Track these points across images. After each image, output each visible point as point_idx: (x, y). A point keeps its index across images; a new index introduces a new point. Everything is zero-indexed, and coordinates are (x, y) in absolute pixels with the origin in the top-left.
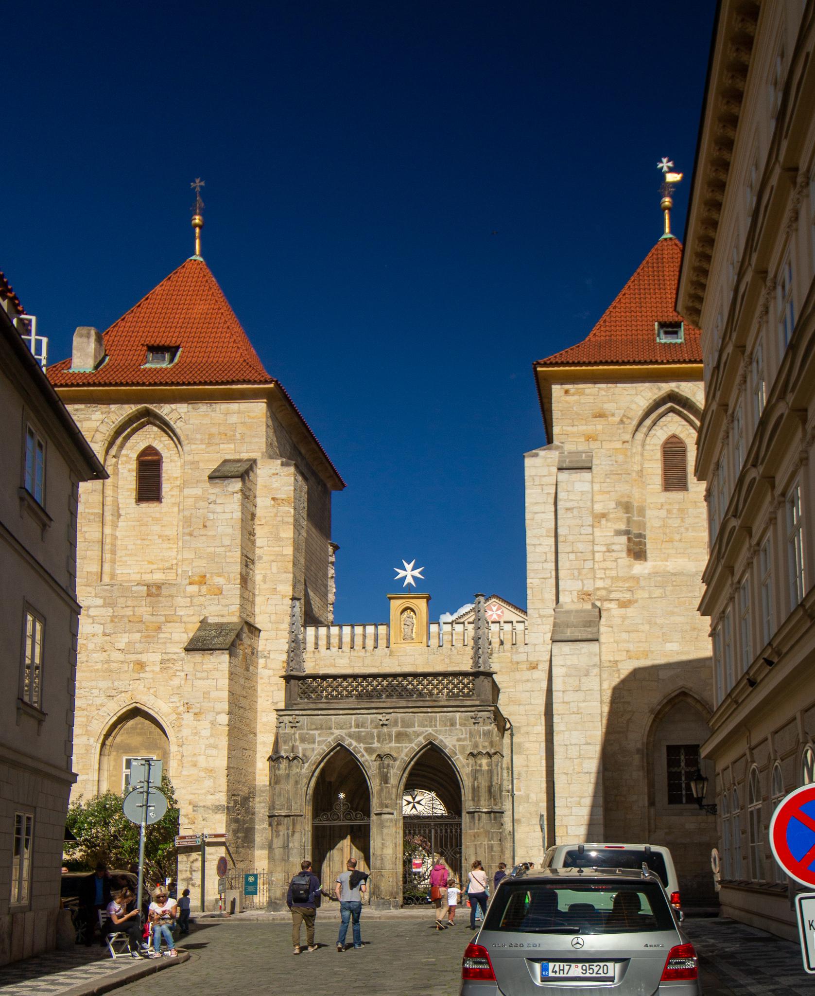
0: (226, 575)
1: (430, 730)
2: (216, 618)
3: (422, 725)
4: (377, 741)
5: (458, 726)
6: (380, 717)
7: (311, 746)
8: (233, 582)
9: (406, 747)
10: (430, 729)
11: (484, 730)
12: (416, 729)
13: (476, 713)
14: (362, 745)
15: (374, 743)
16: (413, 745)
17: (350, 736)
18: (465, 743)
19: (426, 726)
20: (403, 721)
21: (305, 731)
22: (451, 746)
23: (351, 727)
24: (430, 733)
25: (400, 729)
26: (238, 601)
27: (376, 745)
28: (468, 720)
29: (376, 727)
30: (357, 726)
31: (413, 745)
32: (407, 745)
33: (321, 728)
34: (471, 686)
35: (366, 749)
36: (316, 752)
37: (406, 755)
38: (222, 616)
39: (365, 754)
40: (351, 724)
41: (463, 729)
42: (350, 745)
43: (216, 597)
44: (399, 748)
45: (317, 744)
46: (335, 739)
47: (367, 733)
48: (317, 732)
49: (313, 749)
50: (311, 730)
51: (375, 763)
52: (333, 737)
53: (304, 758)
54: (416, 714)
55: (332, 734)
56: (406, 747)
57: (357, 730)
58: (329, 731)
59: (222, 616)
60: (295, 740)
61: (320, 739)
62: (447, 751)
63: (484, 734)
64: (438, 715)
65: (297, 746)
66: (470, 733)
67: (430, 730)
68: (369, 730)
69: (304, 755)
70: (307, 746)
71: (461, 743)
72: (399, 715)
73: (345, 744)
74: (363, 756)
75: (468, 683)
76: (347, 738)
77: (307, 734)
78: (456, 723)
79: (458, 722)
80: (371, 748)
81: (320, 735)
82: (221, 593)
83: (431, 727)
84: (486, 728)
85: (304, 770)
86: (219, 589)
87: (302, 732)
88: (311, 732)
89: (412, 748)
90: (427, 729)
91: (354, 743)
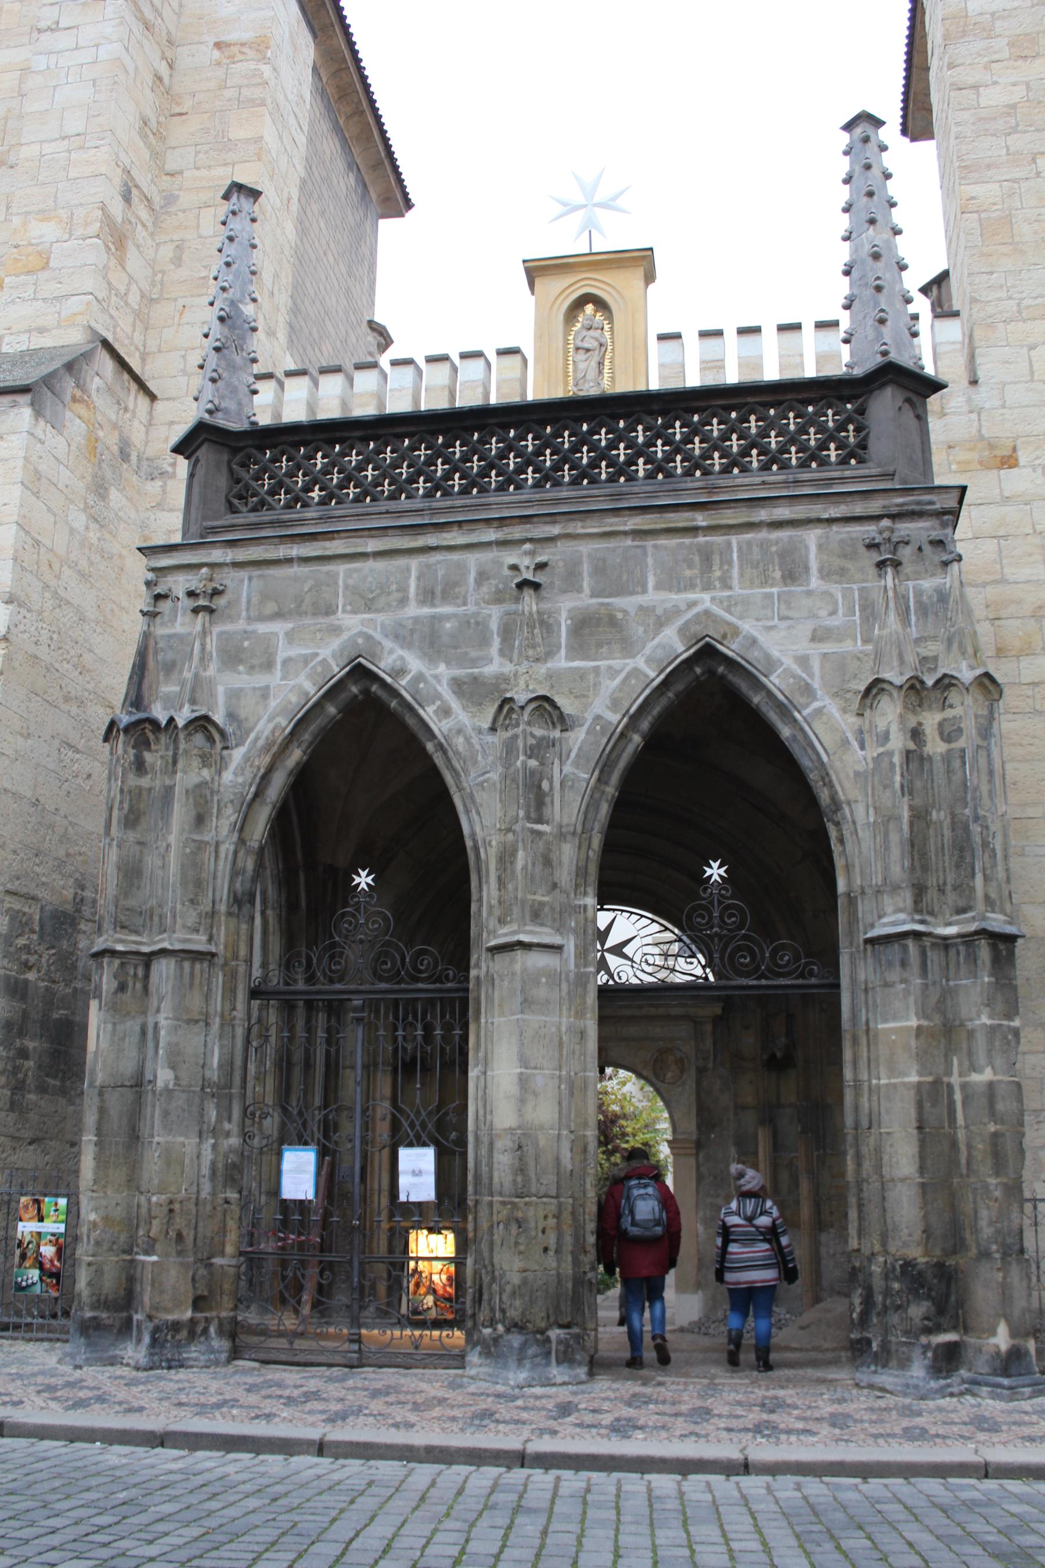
0: (63, 214)
1: (705, 600)
2: (24, 337)
3: (671, 582)
4: (502, 653)
5: (815, 582)
6: (511, 557)
7: (261, 680)
8: (79, 232)
9: (613, 672)
10: (706, 597)
11: (919, 593)
12: (653, 597)
13: (886, 523)
14: (442, 668)
15: (491, 661)
16: (640, 662)
17: (401, 635)
18: (847, 646)
19: (691, 586)
20: (600, 569)
21: (241, 625)
22: (788, 662)
23: (403, 601)
24: (707, 613)
25: (585, 600)
26: (89, 283)
27: (495, 666)
28: (852, 556)
29: (498, 598)
30: (428, 596)
31: (640, 662)
32: (616, 663)
33: (298, 612)
34: (851, 436)
35: (458, 686)
36: (273, 703)
37: (614, 704)
38: (42, 331)
39: (455, 704)
40: (403, 589)
41: (836, 590)
42: (399, 672)
43: (31, 279)
44: (581, 675)
45: (278, 672)
46: (342, 650)
47: (465, 622)
48: (279, 628)
49: (265, 693)
50: (262, 618)
51: (490, 738)
52: (336, 643)
53: (229, 730)
54: (650, 543)
55: (336, 630)
56: (613, 672)
57: (426, 611)
58: (323, 620)
59: (42, 331)
60: (204, 658)
61: (294, 652)
62: (774, 681)
63: (923, 610)
64: (734, 540)
65: (211, 681)
66: (863, 609)
67: (705, 600)
68: (471, 608)
69: (231, 716)
70: (242, 679)
71: (829, 647)
72: (585, 548)
73: (383, 666)
74: (446, 712)
75: (842, 427)
76: (388, 644)
77: (246, 634)
78: (807, 569)
79: (814, 565)
80: (475, 679)
81: (290, 636)
82: (46, 266)
83: (707, 587)
84: (928, 584)
85: (228, 776)
86: (39, 253)
87: (229, 627)
88: (262, 628)
89: (636, 672)
90: (692, 596)
91: (415, 664)
